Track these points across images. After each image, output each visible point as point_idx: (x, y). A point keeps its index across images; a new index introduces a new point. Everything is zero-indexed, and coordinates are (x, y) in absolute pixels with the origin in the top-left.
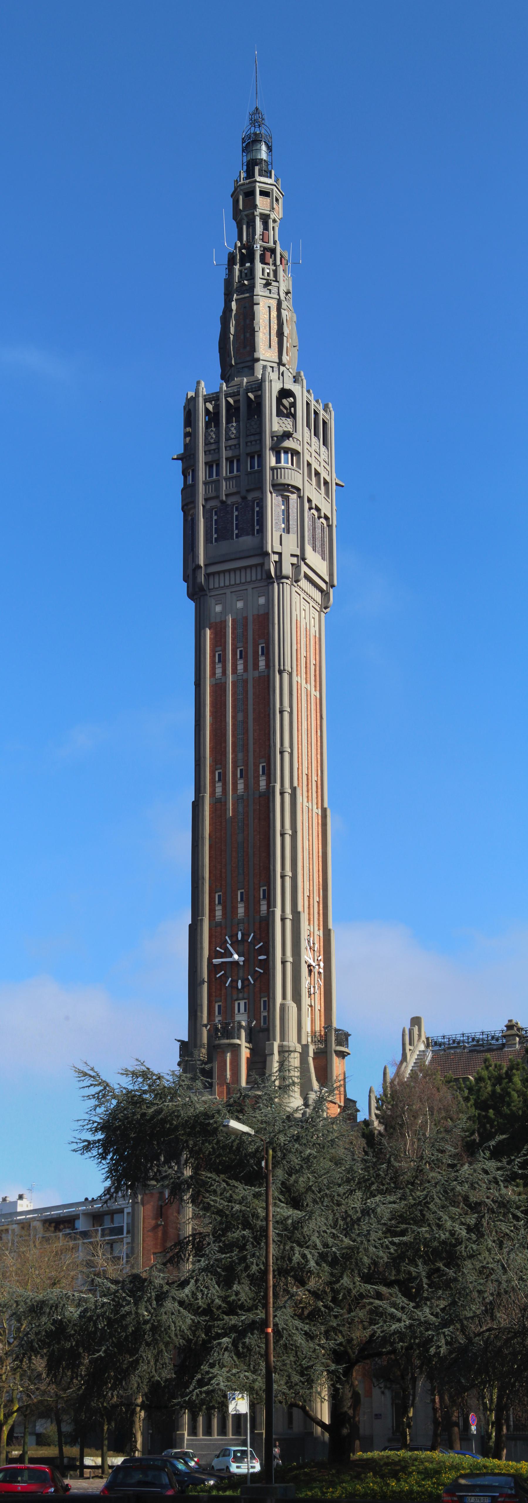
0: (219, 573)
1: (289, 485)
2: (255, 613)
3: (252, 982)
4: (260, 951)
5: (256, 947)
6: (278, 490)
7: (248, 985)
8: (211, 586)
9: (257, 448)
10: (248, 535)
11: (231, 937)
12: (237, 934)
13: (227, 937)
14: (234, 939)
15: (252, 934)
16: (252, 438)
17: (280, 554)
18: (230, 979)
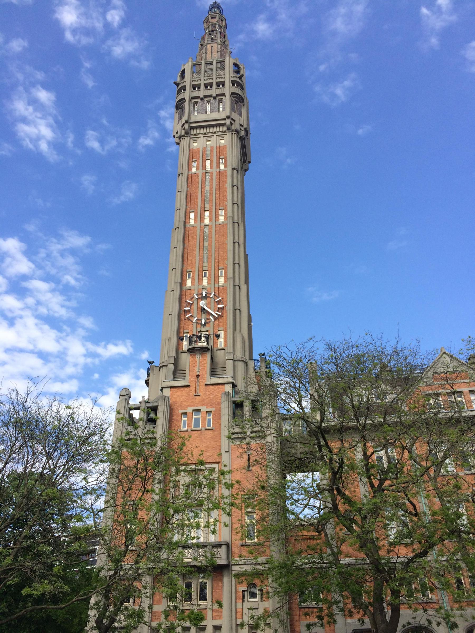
0: (197, 128)
1: (240, 95)
2: (218, 145)
3: (213, 320)
4: (219, 302)
5: (216, 300)
6: (233, 97)
7: (209, 322)
8: (192, 133)
9: (222, 80)
10: (216, 111)
11: (198, 295)
12: (202, 294)
13: (195, 295)
14: (200, 296)
15: (213, 293)
16: (220, 76)
17: (234, 121)
18: (196, 318)
